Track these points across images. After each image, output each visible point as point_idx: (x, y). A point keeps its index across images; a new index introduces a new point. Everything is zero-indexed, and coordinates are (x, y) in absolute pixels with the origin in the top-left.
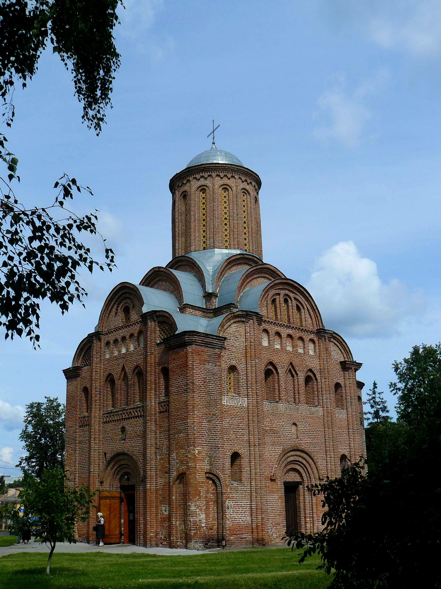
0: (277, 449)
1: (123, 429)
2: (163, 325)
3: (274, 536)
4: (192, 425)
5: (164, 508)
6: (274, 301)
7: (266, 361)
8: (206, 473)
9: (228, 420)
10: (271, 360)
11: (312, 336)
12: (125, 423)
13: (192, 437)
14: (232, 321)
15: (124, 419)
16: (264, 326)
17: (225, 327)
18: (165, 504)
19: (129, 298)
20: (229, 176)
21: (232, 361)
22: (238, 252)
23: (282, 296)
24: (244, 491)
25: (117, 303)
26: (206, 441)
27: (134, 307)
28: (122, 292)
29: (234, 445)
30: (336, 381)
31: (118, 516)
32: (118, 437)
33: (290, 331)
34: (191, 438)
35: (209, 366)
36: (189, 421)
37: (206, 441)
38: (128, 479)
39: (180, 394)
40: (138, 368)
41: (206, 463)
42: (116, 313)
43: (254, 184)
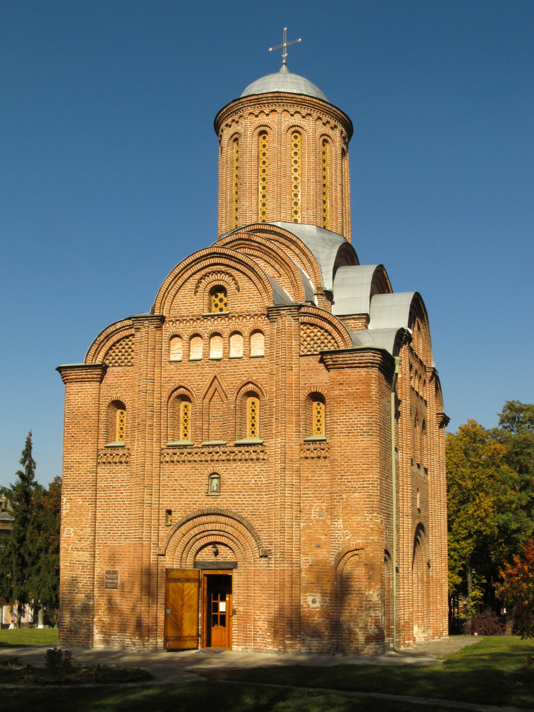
1: (213, 475)
2: (308, 328)
4: (376, 483)
5: (310, 599)
12: (219, 468)
13: (376, 500)
15: (218, 461)
18: (312, 592)
19: (227, 274)
25: (198, 276)
27: (238, 289)
28: (212, 261)
31: (195, 607)
32: (202, 488)
34: (374, 501)
36: (371, 476)
38: (216, 553)
39: (352, 436)
40: (250, 385)
42: (196, 292)
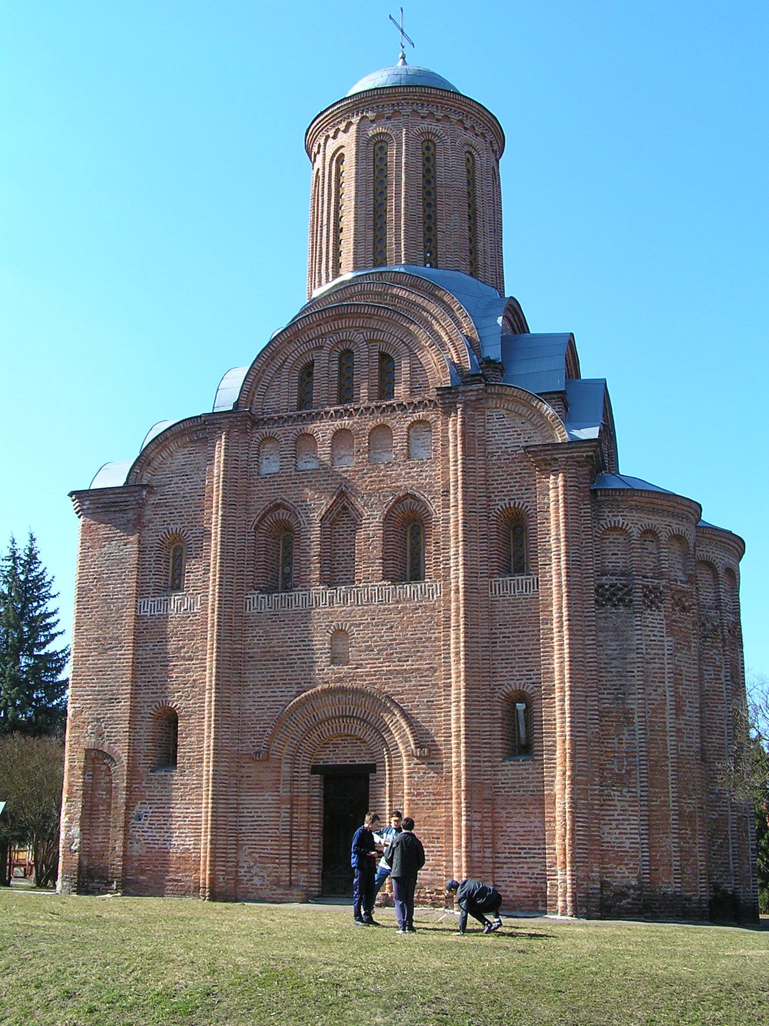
0: (281, 694)
3: (256, 881)
6: (311, 365)
7: (262, 507)
8: (87, 751)
9: (151, 645)
10: (279, 501)
11: (420, 414)
14: (173, 446)
16: (266, 431)
17: (155, 464)
20: (342, 126)
21: (172, 526)
23: (326, 350)
24: (182, 785)
26: (91, 691)
29: (163, 693)
33: (346, 422)
35: (111, 548)
37: (91, 691)
41: (90, 731)
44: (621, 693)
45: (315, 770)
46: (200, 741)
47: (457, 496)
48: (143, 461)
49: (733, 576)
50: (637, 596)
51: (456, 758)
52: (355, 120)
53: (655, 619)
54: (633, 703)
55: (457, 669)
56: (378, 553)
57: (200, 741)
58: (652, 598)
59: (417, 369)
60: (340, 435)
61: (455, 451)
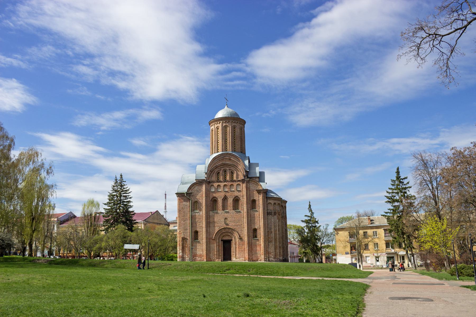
11: (238, 183)
16: (212, 184)
22: (221, 153)
30: (252, 199)
33: (226, 183)
35: (185, 203)
43: (231, 121)
44: (271, 229)
45: (222, 240)
46: (203, 236)
47: (245, 197)
48: (190, 188)
49: (285, 207)
50: (273, 214)
51: (246, 239)
52: (221, 122)
53: (276, 217)
54: (273, 230)
55: (246, 225)
56: (232, 206)
57: (203, 236)
58: (275, 214)
59: (237, 175)
60: (225, 185)
61: (244, 190)
